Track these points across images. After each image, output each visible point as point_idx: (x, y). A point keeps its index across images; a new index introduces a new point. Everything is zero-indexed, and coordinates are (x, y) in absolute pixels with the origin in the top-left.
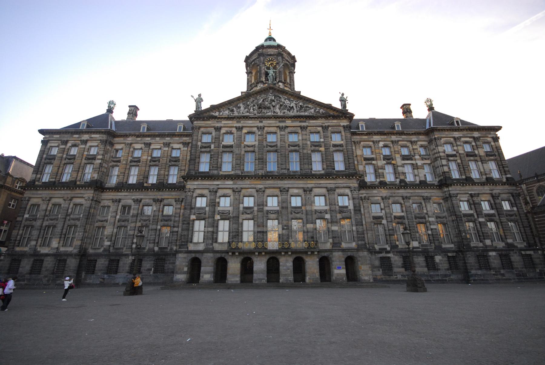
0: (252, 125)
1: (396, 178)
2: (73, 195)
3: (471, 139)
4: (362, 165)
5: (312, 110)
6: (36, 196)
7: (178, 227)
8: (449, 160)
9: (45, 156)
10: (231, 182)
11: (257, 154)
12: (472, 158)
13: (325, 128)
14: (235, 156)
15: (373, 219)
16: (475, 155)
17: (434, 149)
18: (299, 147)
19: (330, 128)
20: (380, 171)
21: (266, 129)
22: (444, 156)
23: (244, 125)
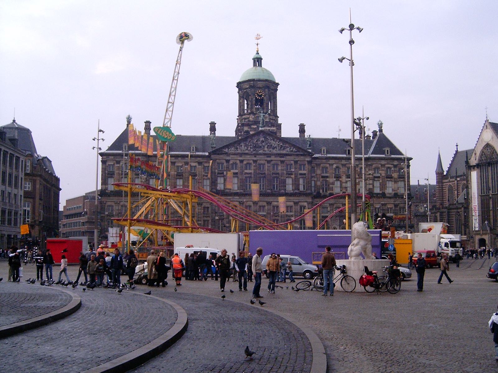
0: (249, 159)
1: (341, 191)
2: (133, 200)
3: (392, 166)
4: (319, 181)
5: (289, 149)
6: (109, 200)
7: (201, 221)
8: (374, 180)
9: (107, 172)
10: (238, 198)
11: (253, 179)
12: (389, 179)
13: (296, 162)
14: (239, 180)
15: (322, 217)
16: (392, 178)
17: (367, 172)
18: (279, 174)
19: (299, 162)
20: (331, 186)
21: (258, 161)
22: (372, 178)
23: (244, 158)
